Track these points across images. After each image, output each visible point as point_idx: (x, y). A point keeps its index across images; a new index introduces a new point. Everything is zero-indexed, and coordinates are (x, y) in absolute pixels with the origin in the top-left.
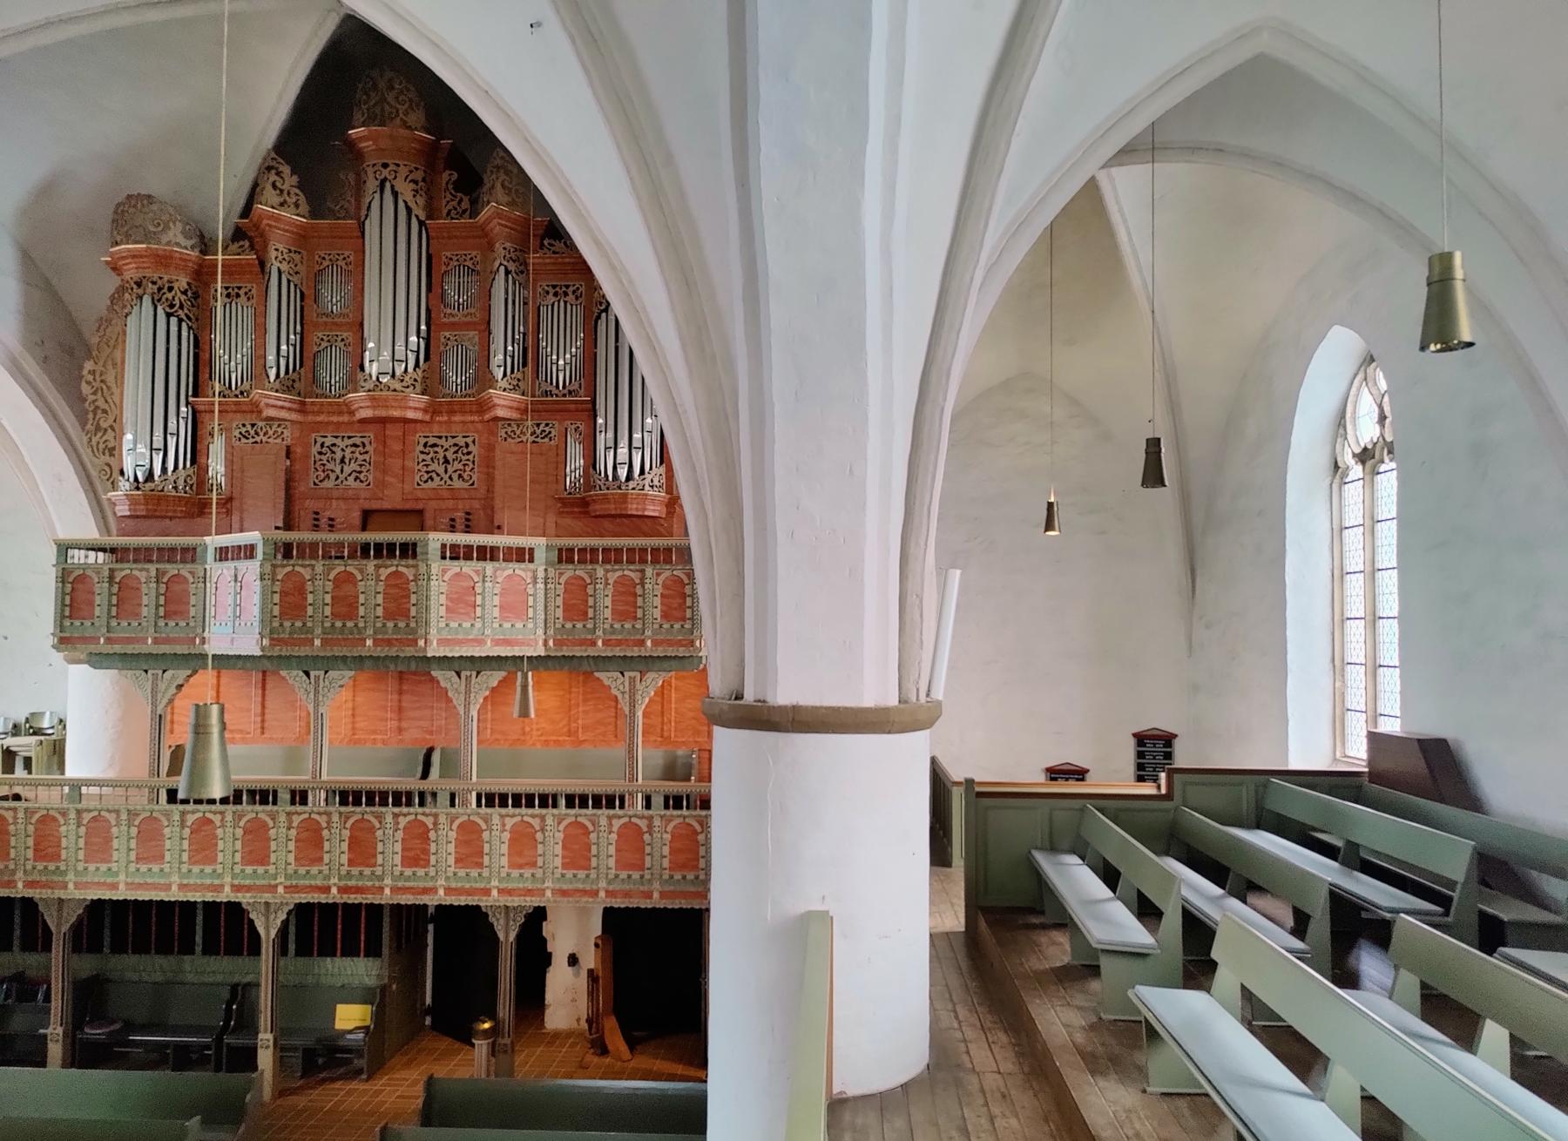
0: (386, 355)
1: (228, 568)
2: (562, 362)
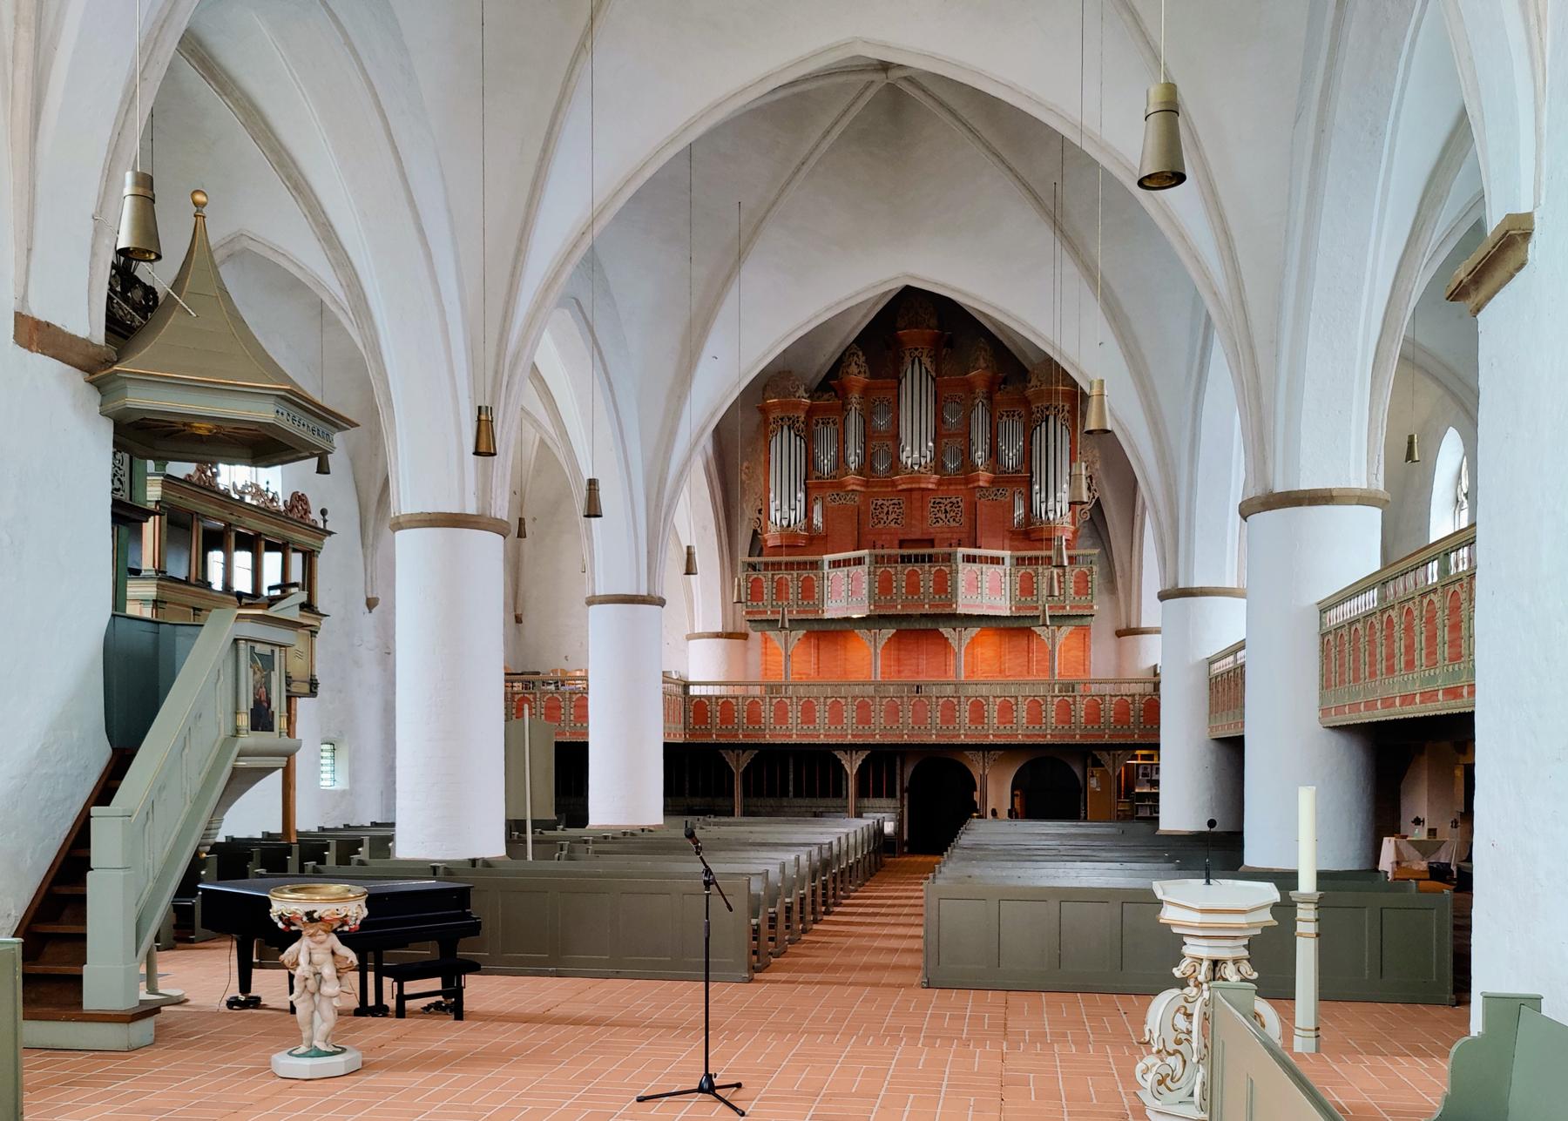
0: (916, 455)
1: (834, 573)
2: (1011, 457)
